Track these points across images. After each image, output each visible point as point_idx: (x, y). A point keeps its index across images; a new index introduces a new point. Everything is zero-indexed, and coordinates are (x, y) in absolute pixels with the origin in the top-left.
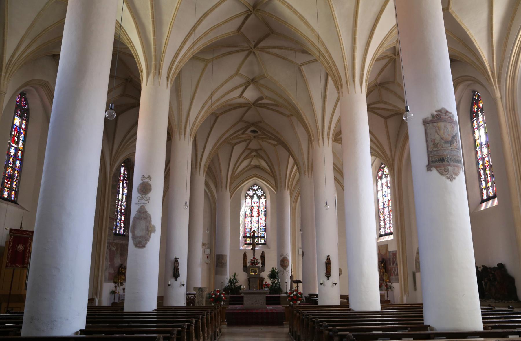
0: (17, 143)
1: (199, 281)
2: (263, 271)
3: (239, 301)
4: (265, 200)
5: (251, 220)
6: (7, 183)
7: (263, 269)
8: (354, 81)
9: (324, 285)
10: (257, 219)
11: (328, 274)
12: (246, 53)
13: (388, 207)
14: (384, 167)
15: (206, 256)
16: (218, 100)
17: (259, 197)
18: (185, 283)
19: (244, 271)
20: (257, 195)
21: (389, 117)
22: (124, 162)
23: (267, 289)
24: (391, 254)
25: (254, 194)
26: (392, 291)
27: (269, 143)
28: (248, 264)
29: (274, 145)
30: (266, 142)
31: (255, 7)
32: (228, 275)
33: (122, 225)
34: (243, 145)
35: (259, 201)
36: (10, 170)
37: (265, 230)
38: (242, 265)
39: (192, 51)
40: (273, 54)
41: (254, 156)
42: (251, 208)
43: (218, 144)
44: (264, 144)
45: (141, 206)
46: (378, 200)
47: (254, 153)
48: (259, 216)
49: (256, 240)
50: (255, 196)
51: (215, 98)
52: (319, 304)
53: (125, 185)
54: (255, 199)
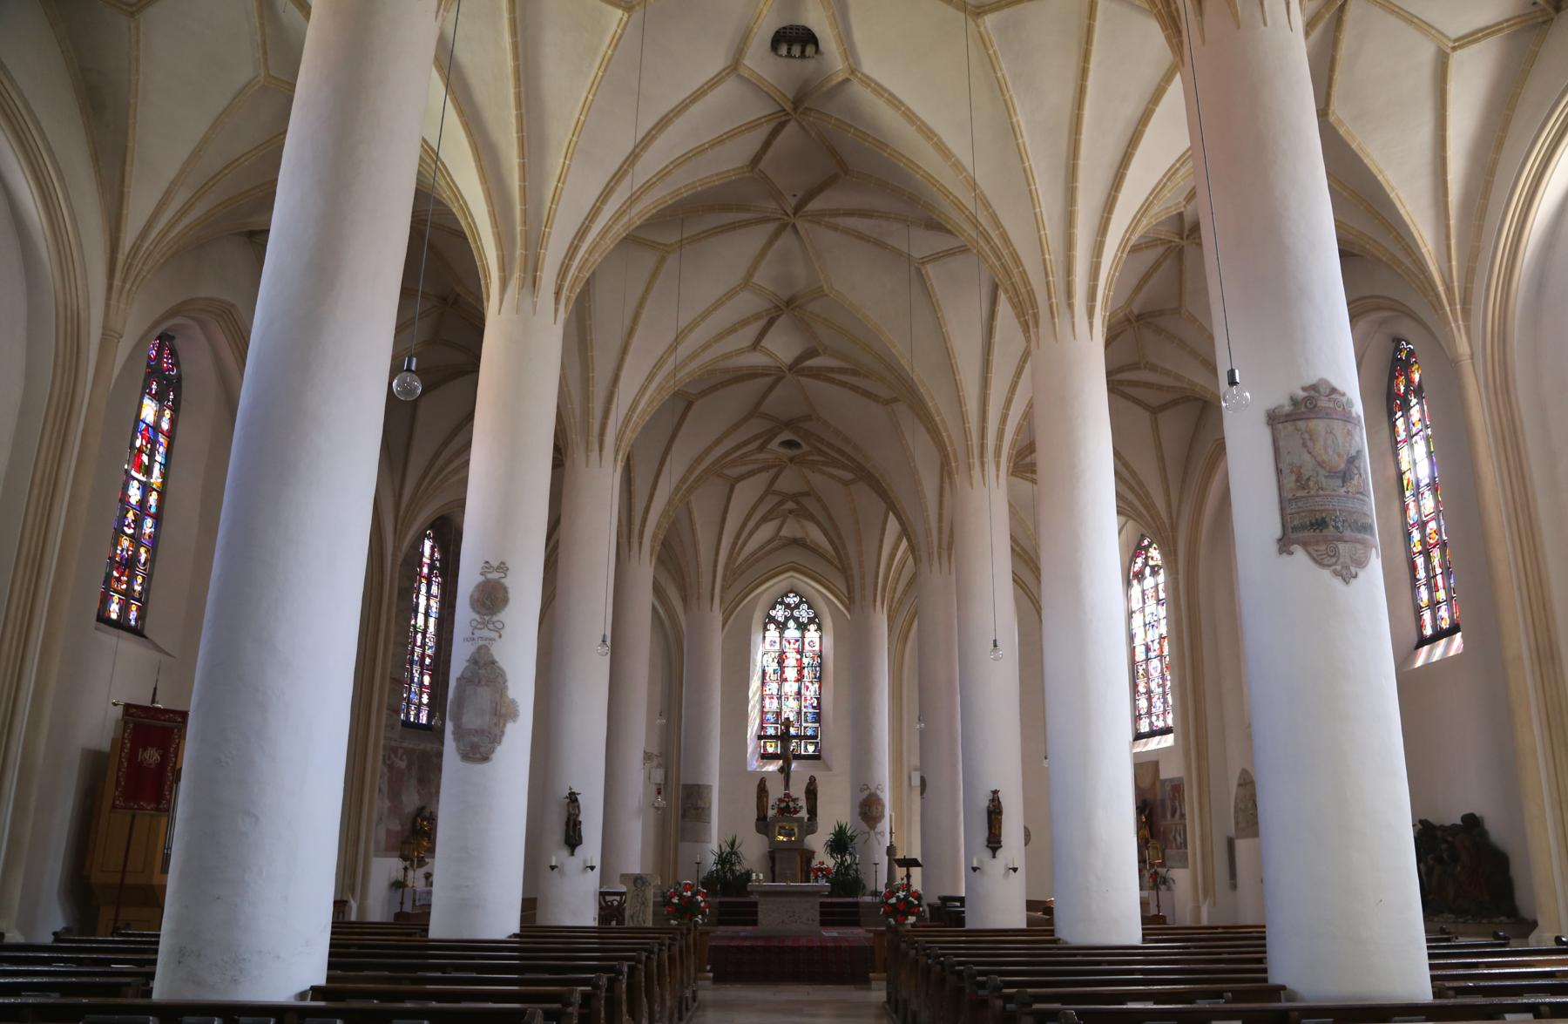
0: (148, 471)
1: (635, 858)
2: (813, 832)
3: (748, 914)
4: (817, 635)
5: (779, 689)
6: (118, 580)
7: (811, 826)
8: (1070, 306)
10: (795, 686)
12: (771, 227)
13: (1161, 656)
14: (1150, 545)
15: (654, 788)
16: (693, 356)
17: (802, 627)
18: (597, 863)
19: (758, 831)
20: (796, 620)
21: (1163, 408)
22: (431, 527)
23: (823, 883)
24: (1168, 788)
25: (787, 619)
26: (1169, 889)
27: (832, 476)
28: (771, 813)
29: (846, 483)
30: (823, 473)
31: (797, 102)
32: (714, 844)
33: (425, 699)
34: (761, 481)
35: (803, 637)
36: (126, 543)
37: (818, 718)
38: (753, 814)
39: (626, 219)
40: (846, 231)
41: (791, 512)
43: (692, 478)
44: (817, 480)
45: (480, 648)
46: (1131, 637)
47: (790, 505)
48: (800, 679)
49: (794, 743)
50: (791, 624)
51: (684, 350)
52: (968, 927)
53: (435, 590)
54: (792, 632)
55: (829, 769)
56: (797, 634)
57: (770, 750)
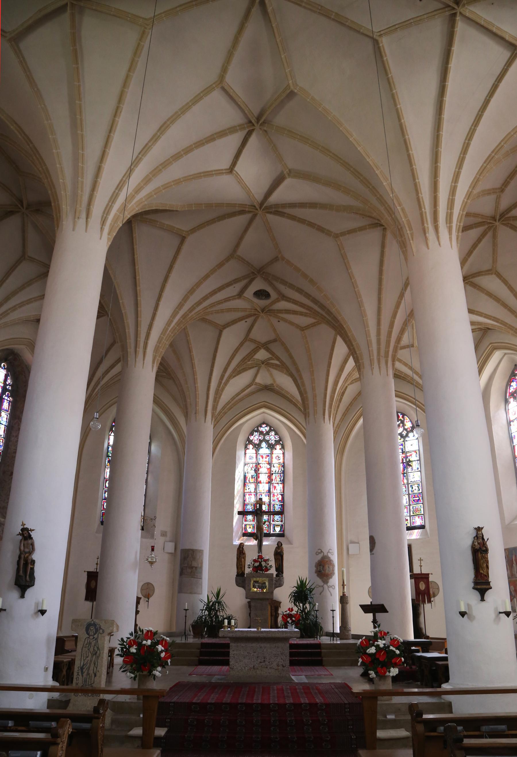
4: (281, 452)
7: (278, 580)
9: (471, 618)
10: (266, 487)
11: (482, 585)
17: (271, 447)
20: (267, 442)
25: (261, 441)
28: (248, 570)
32: (205, 593)
35: (272, 453)
38: (234, 571)
42: (256, 466)
47: (262, 355)
48: (270, 482)
50: (264, 445)
54: (264, 450)
55: (290, 543)
56: (268, 451)
57: (249, 530)
